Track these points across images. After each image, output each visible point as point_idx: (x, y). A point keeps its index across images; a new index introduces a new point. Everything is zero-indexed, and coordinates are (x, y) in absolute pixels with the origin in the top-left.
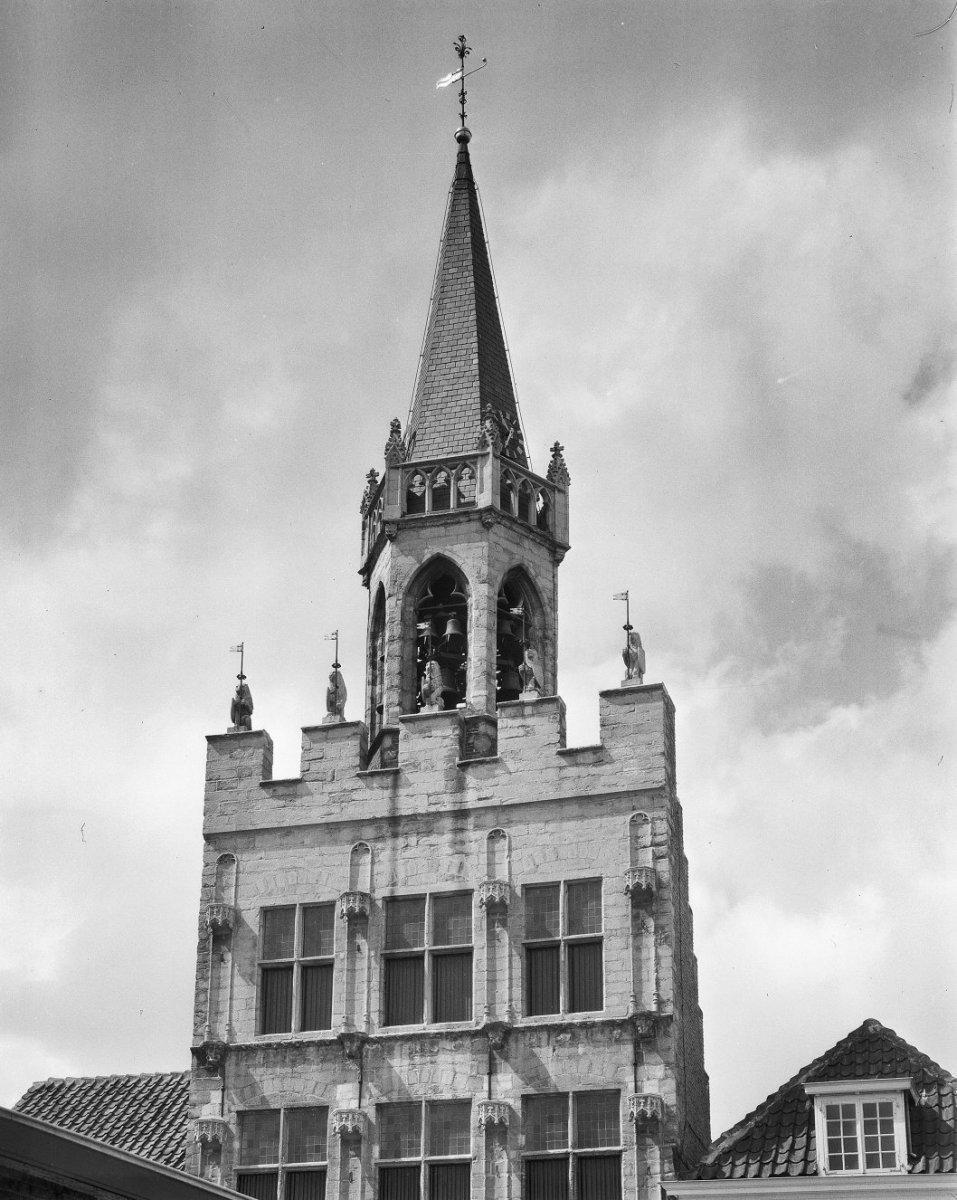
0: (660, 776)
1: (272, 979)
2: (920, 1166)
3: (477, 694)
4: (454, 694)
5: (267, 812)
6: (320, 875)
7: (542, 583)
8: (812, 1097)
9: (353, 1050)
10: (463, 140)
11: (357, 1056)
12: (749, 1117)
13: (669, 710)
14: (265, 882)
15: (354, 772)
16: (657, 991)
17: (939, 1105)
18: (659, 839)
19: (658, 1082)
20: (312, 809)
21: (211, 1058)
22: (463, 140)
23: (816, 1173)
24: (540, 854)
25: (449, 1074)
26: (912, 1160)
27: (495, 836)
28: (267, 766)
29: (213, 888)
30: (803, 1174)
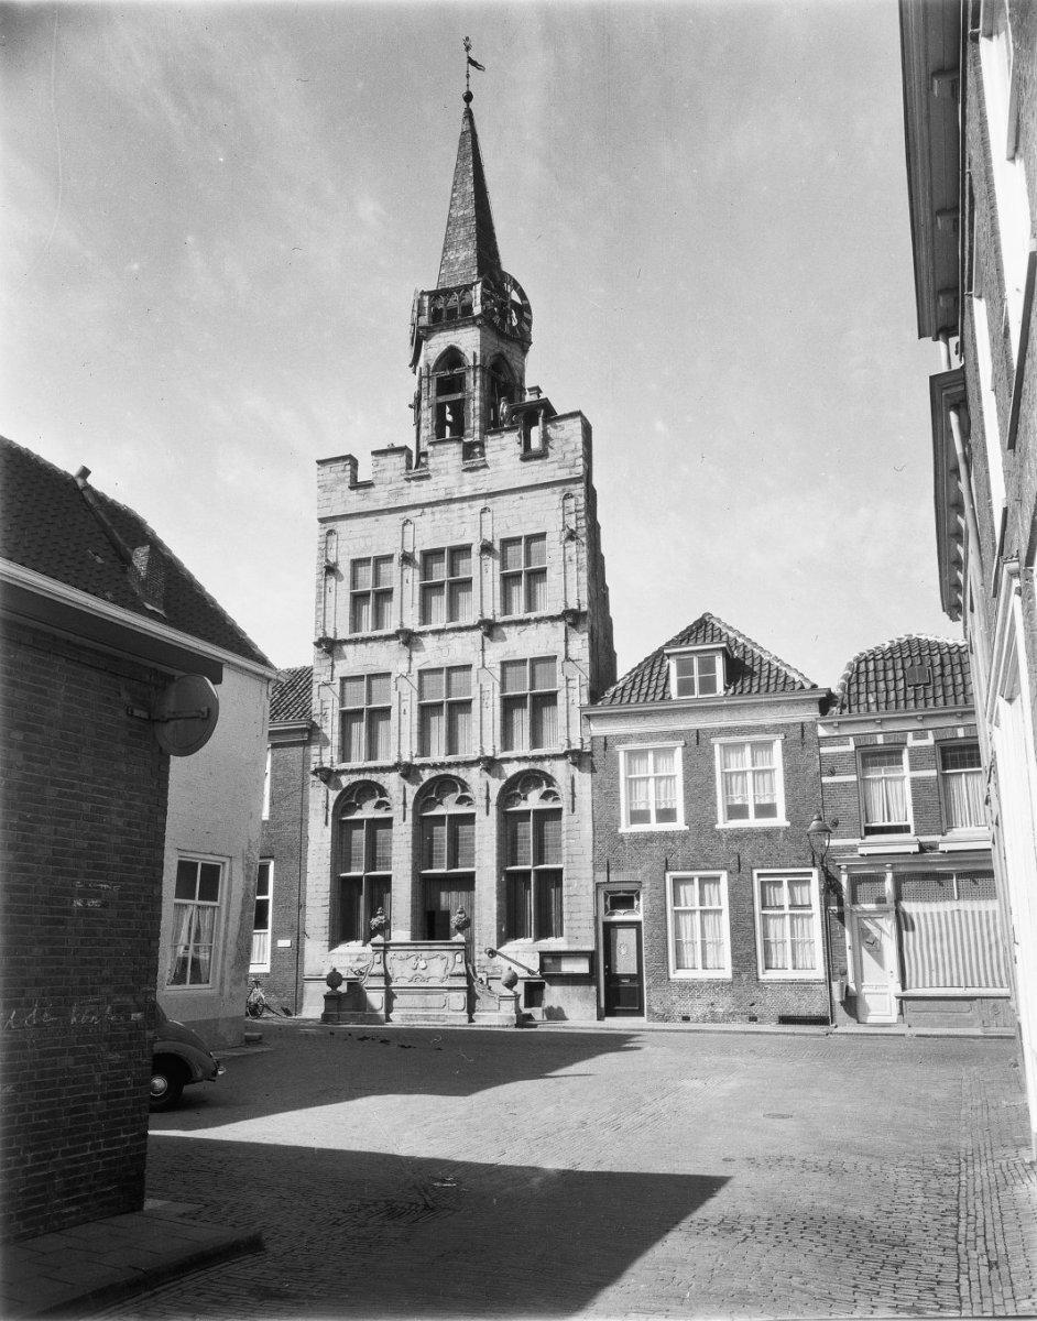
0: (580, 470)
1: (358, 599)
2: (731, 691)
3: (474, 423)
4: (459, 429)
5: (356, 501)
6: (383, 537)
7: (514, 363)
8: (669, 655)
9: (409, 639)
10: (468, 97)
11: (407, 643)
12: (633, 670)
13: (587, 430)
14: (355, 541)
15: (402, 478)
16: (579, 597)
17: (744, 657)
18: (578, 508)
19: (580, 645)
20: (379, 497)
21: (329, 647)
22: (468, 97)
23: (670, 698)
24: (513, 518)
25: (462, 648)
26: (726, 689)
27: (484, 510)
28: (354, 476)
29: (325, 550)
30: (662, 698)
